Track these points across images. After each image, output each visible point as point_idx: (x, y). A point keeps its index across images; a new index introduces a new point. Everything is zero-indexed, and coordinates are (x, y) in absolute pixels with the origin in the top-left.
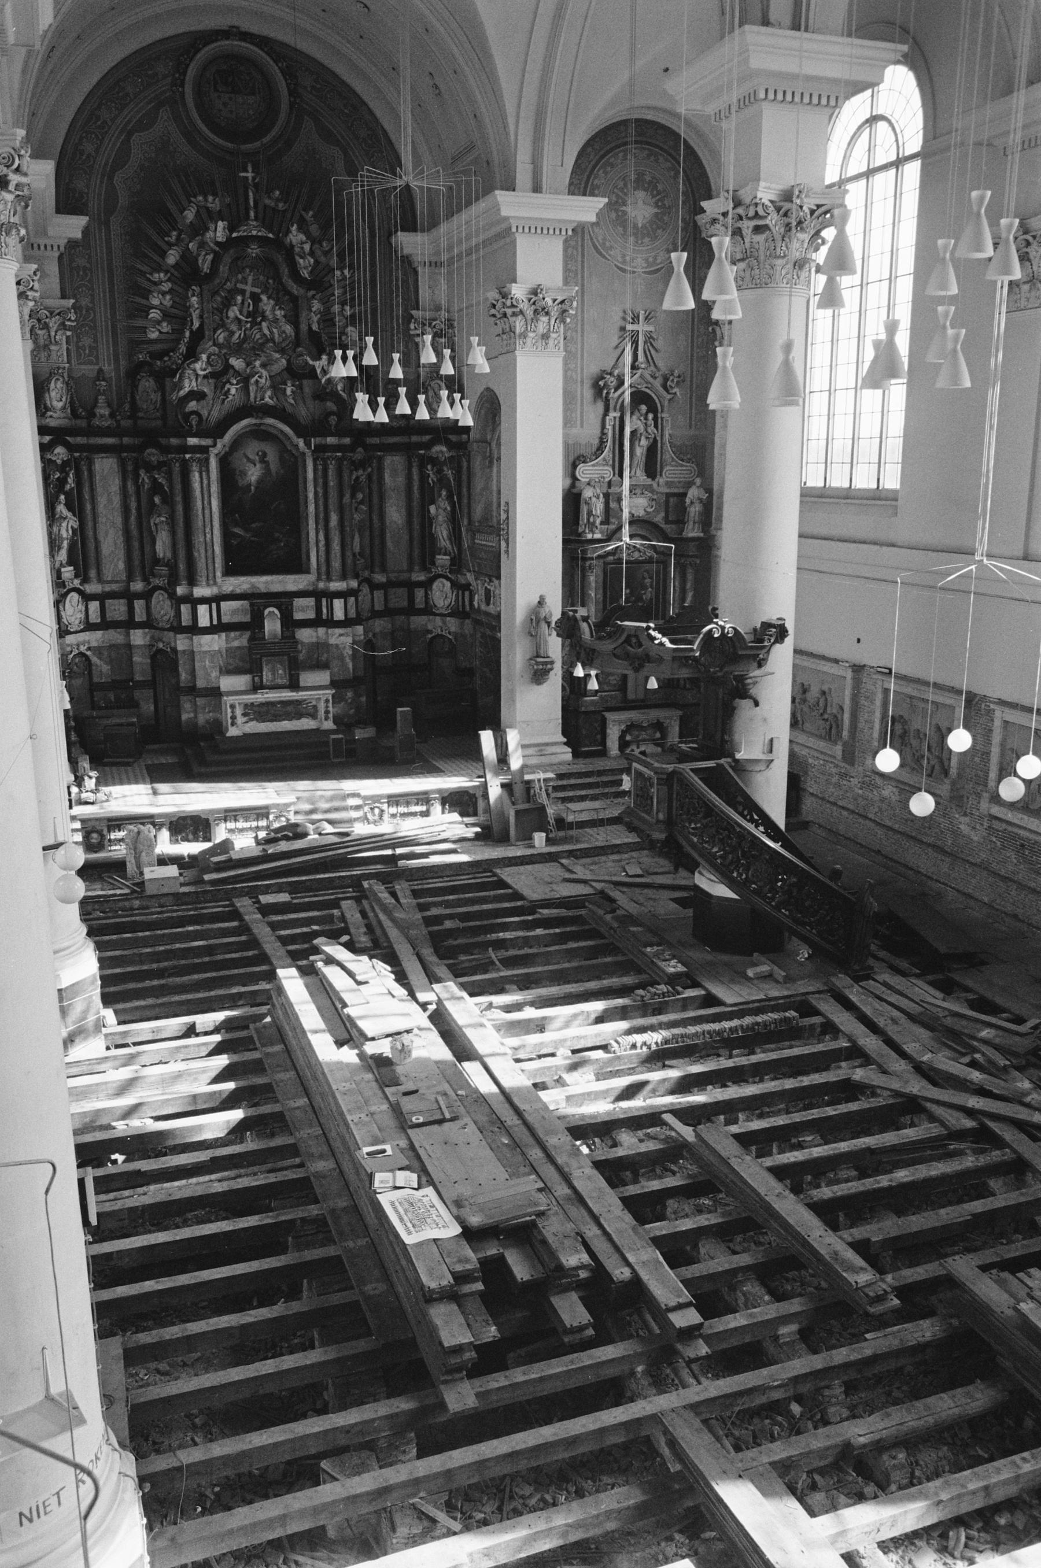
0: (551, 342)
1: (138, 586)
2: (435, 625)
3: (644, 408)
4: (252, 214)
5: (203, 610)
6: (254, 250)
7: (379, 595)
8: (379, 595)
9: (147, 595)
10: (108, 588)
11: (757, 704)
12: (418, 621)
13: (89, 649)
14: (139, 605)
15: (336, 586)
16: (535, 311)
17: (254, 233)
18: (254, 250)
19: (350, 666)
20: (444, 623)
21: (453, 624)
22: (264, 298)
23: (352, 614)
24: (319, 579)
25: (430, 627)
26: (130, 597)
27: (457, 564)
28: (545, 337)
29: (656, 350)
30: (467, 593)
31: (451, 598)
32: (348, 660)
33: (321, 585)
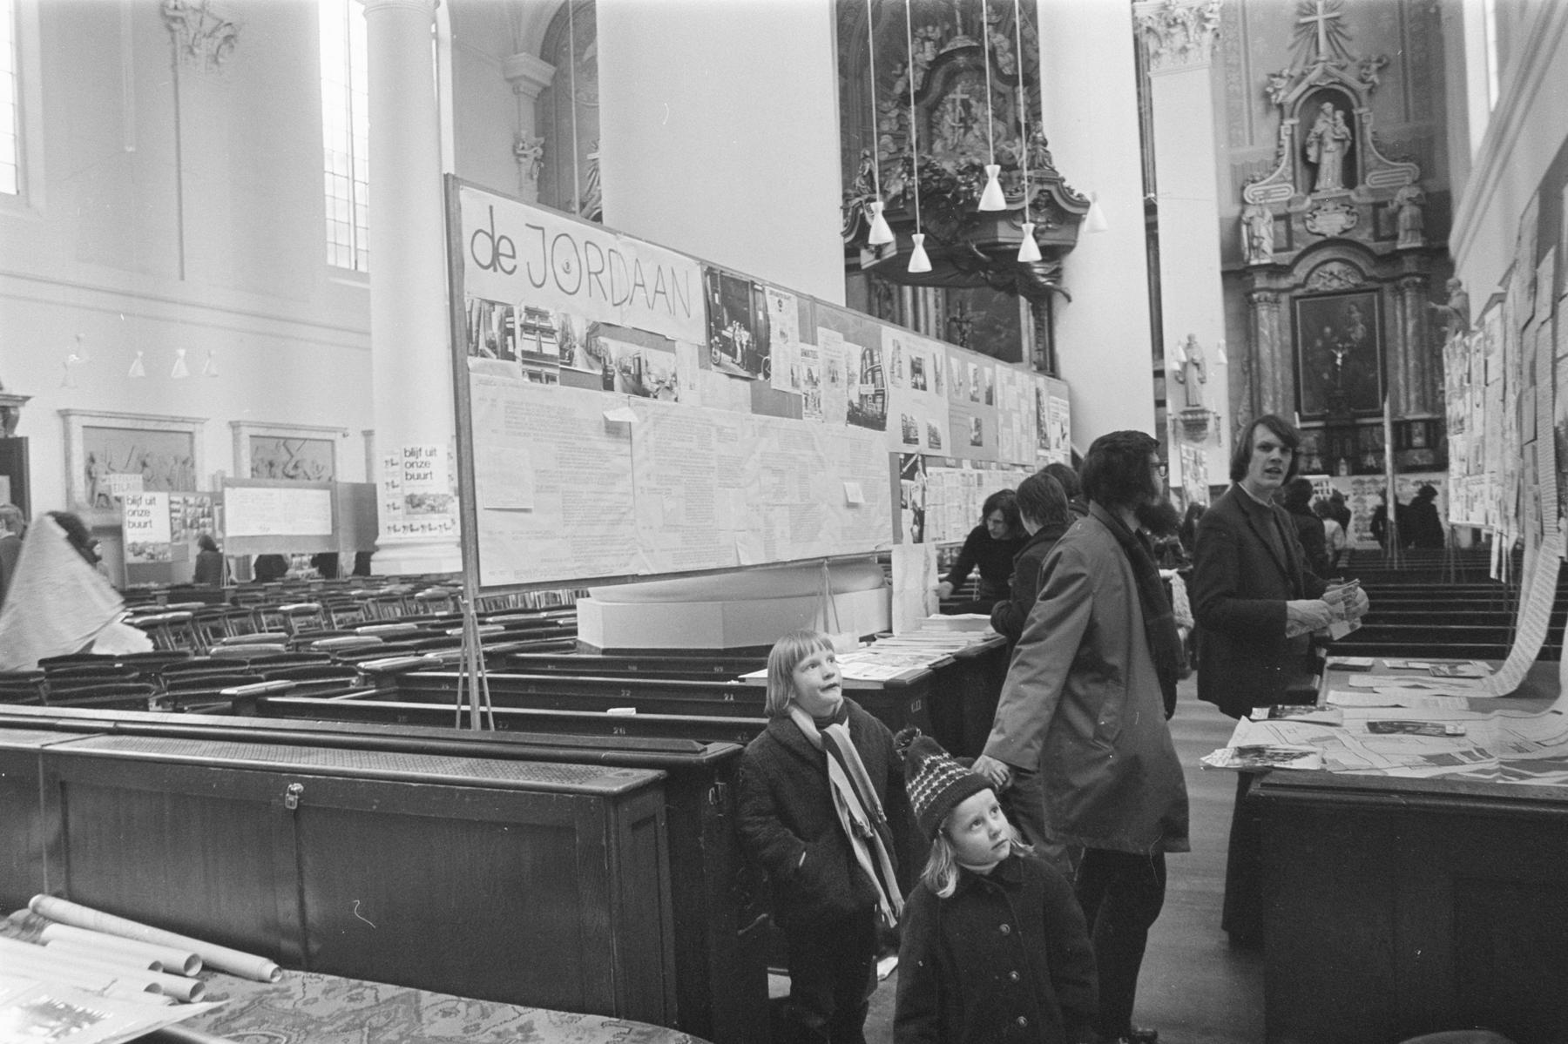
0: (1191, 54)
3: (1328, 106)
4: (960, 30)
6: (961, 60)
11: (1069, 299)
16: (1169, 26)
17: (959, 45)
18: (961, 60)
22: (973, 102)
28: (1184, 50)
29: (1349, 39)
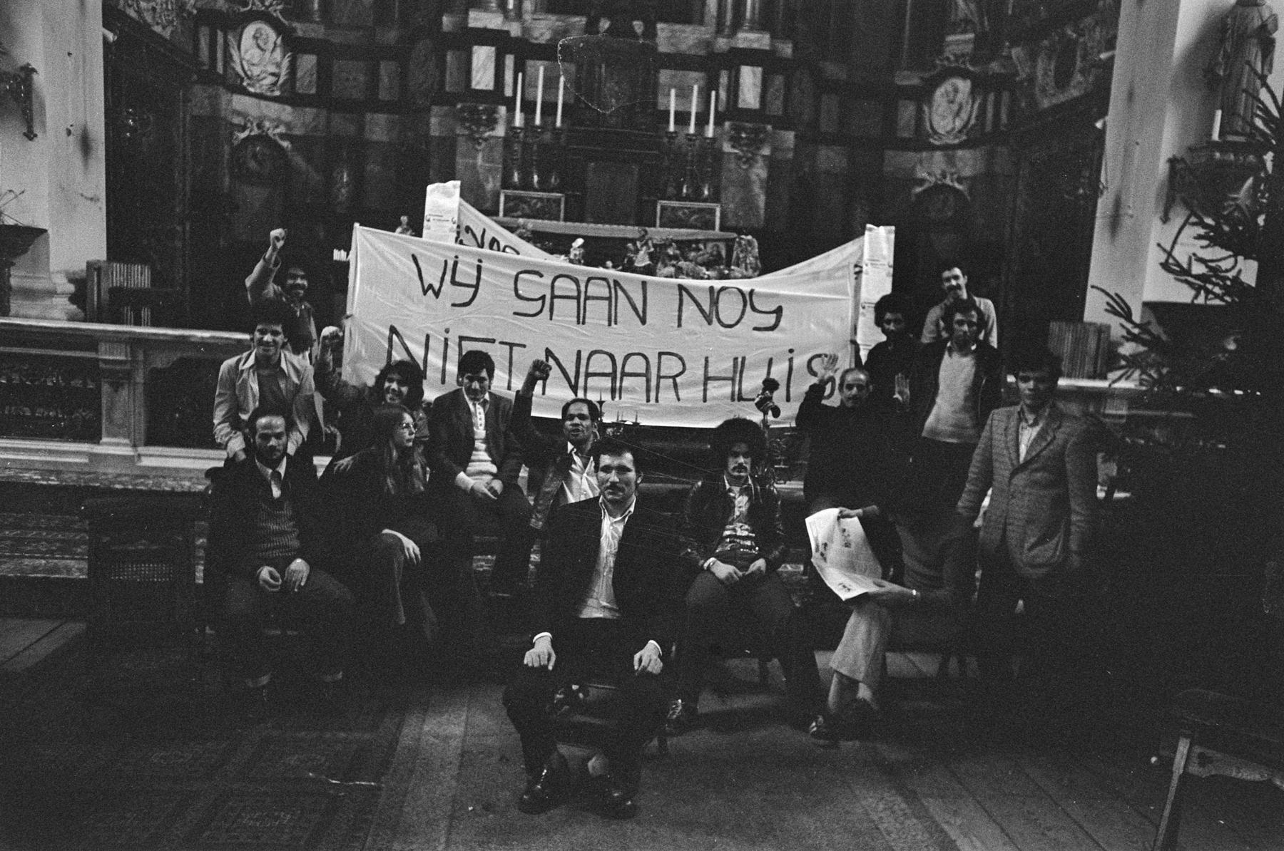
1: (391, 36)
2: (930, 169)
5: (483, 56)
7: (830, 103)
8: (830, 103)
9: (400, 55)
10: (337, 39)
12: (897, 160)
13: (282, 136)
14: (386, 70)
15: (749, 39)
19: (762, 201)
20: (951, 161)
21: (968, 162)
23: (776, 107)
24: (719, 31)
25: (921, 174)
26: (371, 55)
27: (986, 46)
30: (1006, 96)
31: (970, 111)
32: (757, 189)
33: (722, 43)
